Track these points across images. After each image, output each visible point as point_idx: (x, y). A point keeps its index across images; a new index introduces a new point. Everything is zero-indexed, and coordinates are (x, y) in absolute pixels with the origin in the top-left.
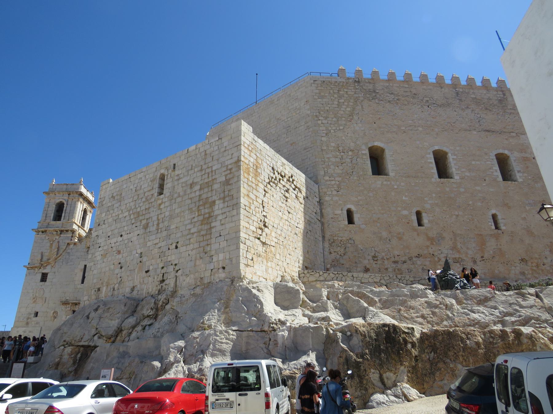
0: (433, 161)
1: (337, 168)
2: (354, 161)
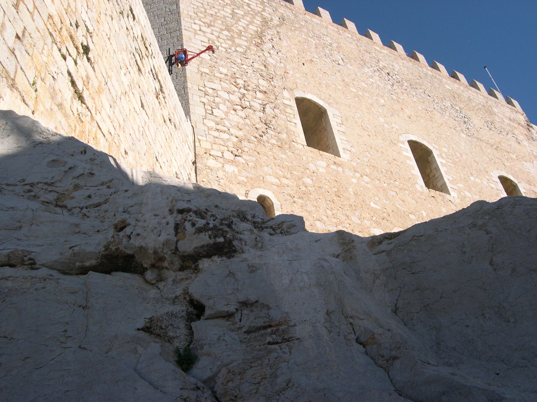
0: (410, 154)
1: (233, 112)
2: (268, 110)
